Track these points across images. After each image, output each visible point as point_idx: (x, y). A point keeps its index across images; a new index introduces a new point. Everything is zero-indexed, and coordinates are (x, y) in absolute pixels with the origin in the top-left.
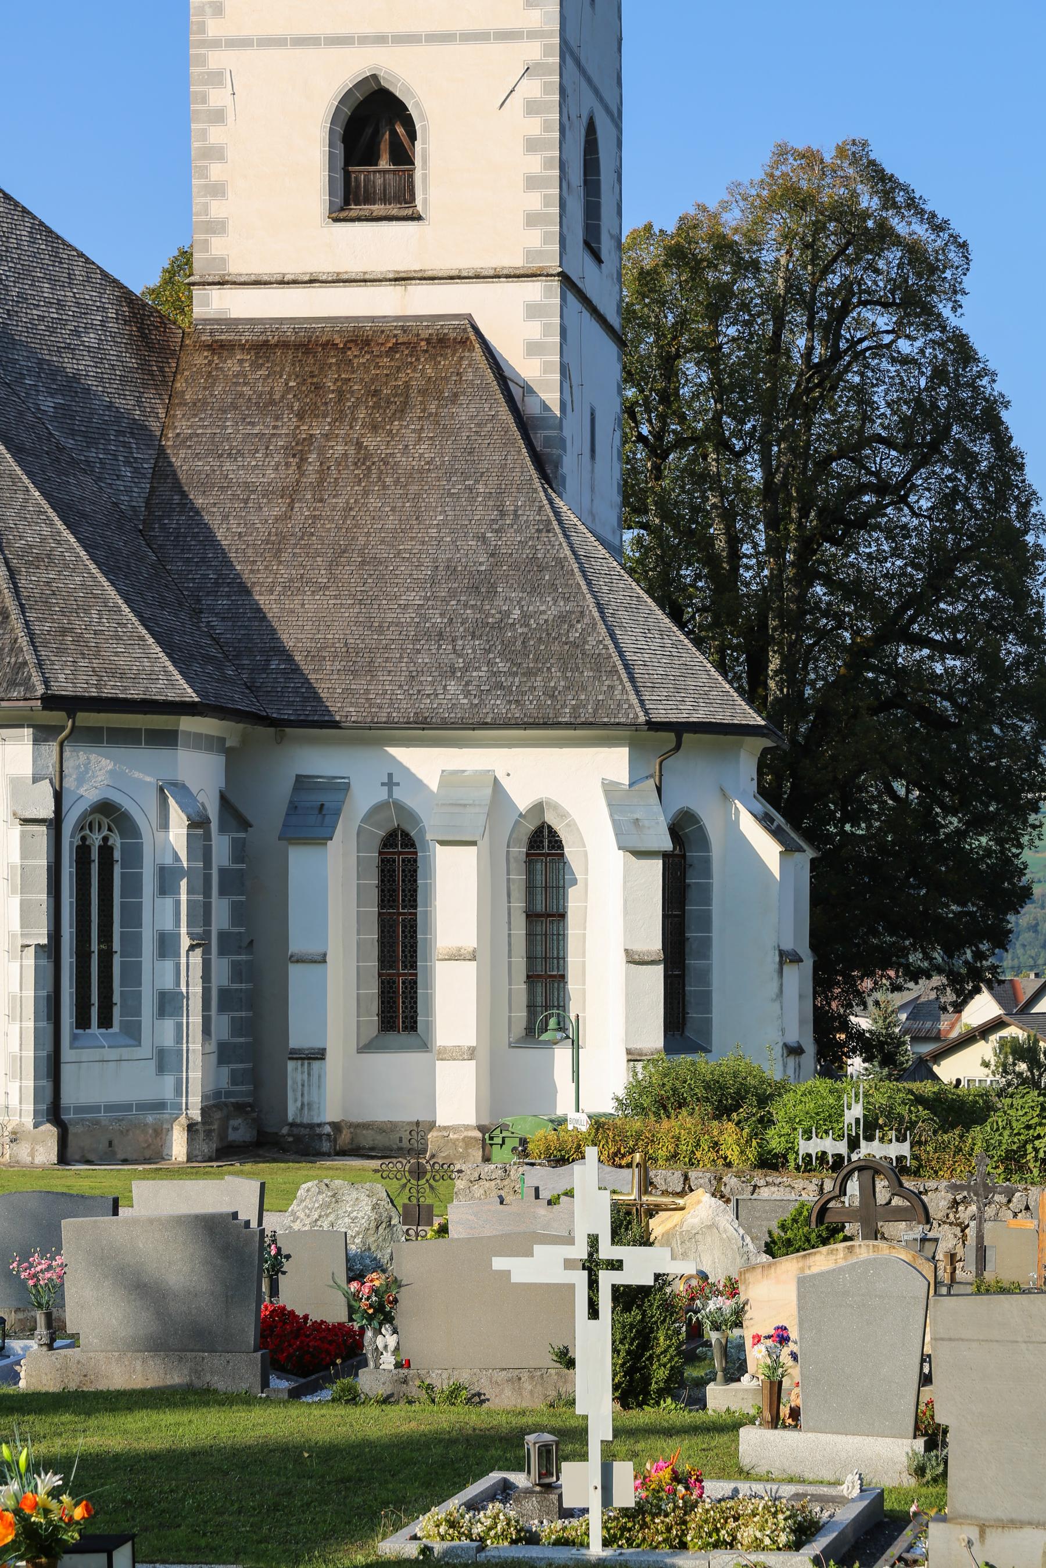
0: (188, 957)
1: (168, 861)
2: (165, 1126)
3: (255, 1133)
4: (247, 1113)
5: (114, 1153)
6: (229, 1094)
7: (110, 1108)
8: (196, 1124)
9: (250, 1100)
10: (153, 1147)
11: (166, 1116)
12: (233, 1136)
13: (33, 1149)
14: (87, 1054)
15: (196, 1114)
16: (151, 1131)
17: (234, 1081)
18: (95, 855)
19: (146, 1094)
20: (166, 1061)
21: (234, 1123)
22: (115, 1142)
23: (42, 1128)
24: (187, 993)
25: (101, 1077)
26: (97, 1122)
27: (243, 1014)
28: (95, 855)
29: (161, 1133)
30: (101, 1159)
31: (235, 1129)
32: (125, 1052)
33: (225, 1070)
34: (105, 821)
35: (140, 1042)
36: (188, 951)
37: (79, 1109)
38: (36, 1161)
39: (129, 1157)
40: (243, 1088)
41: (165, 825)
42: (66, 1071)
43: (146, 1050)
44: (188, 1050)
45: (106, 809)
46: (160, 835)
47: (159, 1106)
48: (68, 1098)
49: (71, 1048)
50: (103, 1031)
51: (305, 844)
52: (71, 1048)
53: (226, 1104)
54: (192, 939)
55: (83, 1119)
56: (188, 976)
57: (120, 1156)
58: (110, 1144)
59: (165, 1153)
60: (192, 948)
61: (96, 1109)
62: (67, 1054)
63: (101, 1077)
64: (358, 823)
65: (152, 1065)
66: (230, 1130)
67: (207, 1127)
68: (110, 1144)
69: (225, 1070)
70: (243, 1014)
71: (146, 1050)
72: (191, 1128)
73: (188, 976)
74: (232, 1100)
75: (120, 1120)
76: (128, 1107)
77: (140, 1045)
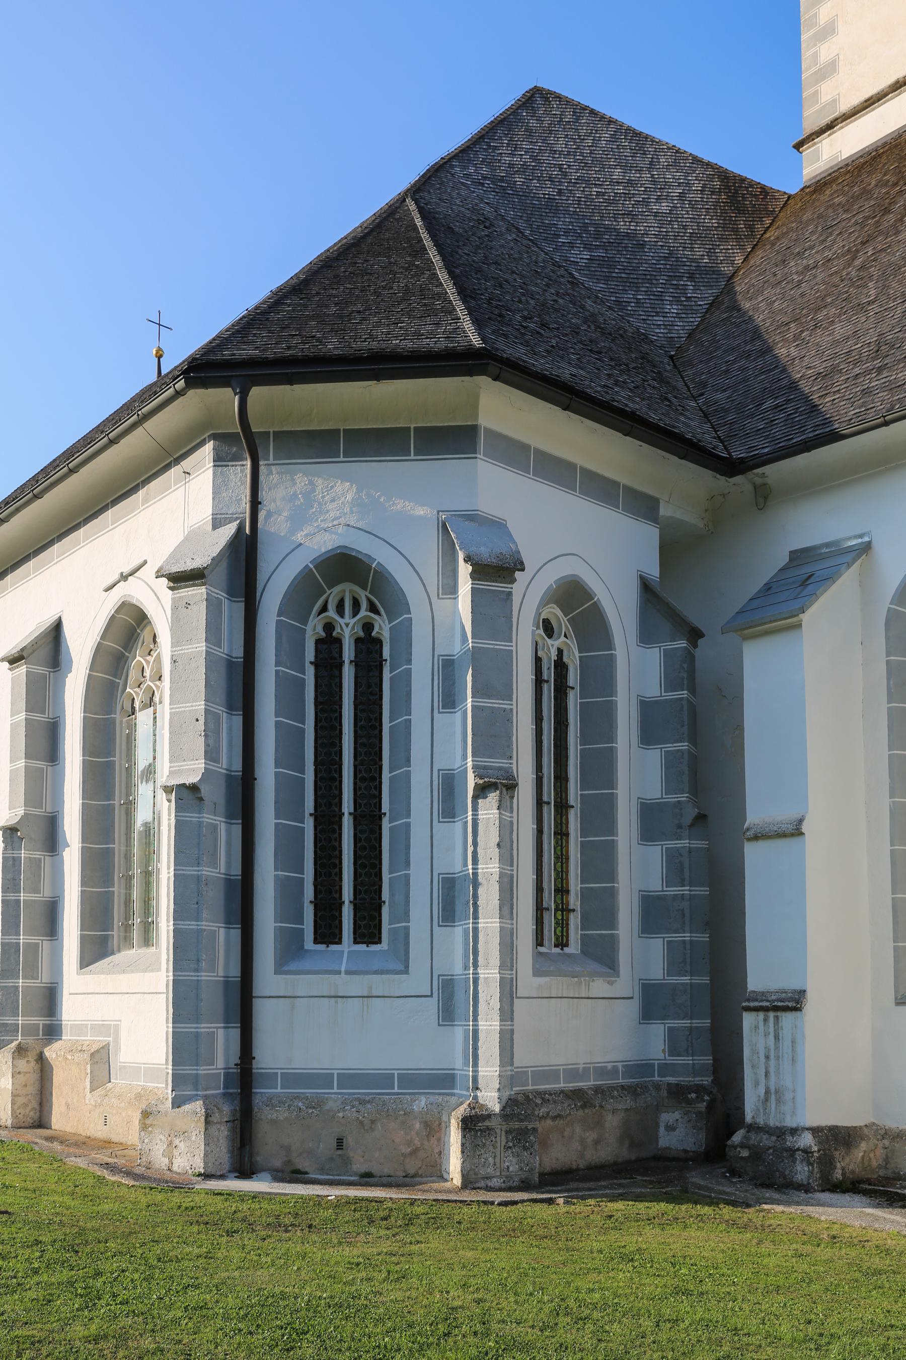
0: (475, 809)
1: (457, 649)
2: (444, 1118)
3: (702, 1136)
4: (689, 1102)
5: (346, 1161)
6: (665, 1069)
7: (349, 1079)
8: (489, 1116)
9: (707, 1080)
10: (422, 1154)
11: (453, 1100)
12: (667, 1140)
13: (171, 1143)
14: (305, 984)
15: (491, 1099)
16: (417, 1126)
17: (673, 1050)
18: (348, 652)
19: (423, 1059)
20: (451, 1000)
21: (666, 1117)
22: (350, 1141)
23: (187, 1107)
24: (475, 875)
25: (327, 1024)
26: (318, 1103)
27: (687, 936)
28: (348, 652)
29: (434, 1129)
30: (322, 1170)
31: (670, 1128)
32: (378, 983)
33: (658, 1032)
34: (363, 596)
35: (407, 967)
36: (476, 797)
37: (294, 1079)
38: (175, 1168)
39: (375, 1169)
40: (687, 1060)
41: (452, 590)
42: (266, 1014)
43: (418, 979)
44: (476, 981)
45: (345, 570)
46: (442, 605)
47: (444, 1081)
48: (271, 1055)
49: (276, 972)
50: (362, 947)
51: (767, 633)
52: (276, 972)
53: (657, 1087)
54: (478, 776)
55: (297, 1097)
56: (475, 844)
57: (360, 1166)
58: (340, 1143)
59: (443, 1168)
60: (482, 791)
61: (324, 1079)
62: (267, 978)
63: (327, 1024)
64: (887, 604)
65: (432, 1006)
66: (662, 1130)
67: (516, 1125)
68: (340, 1143)
69: (658, 1032)
70: (687, 936)
71: (418, 979)
72: (473, 1124)
73: (475, 844)
74: (671, 1080)
75: (362, 1102)
76: (383, 1080)
77: (406, 971)
